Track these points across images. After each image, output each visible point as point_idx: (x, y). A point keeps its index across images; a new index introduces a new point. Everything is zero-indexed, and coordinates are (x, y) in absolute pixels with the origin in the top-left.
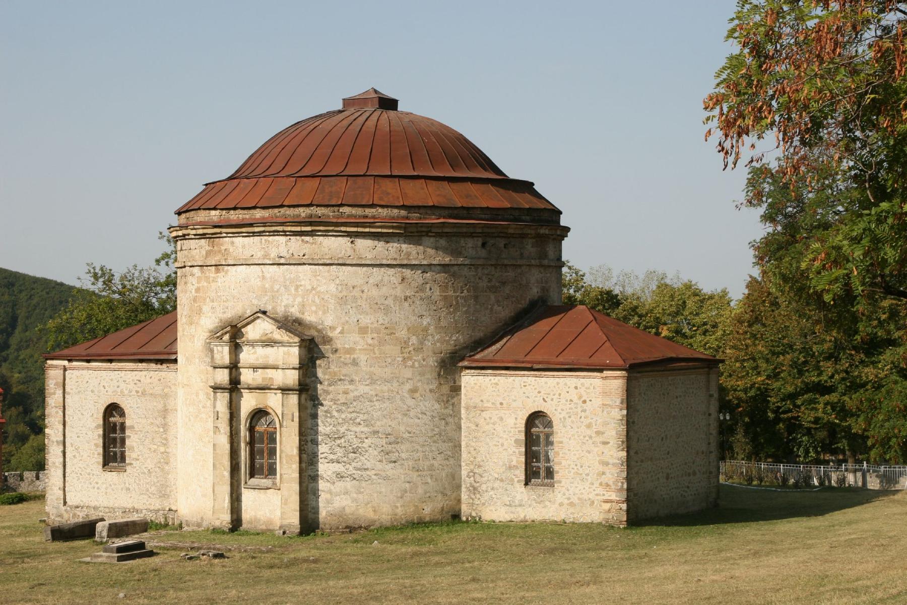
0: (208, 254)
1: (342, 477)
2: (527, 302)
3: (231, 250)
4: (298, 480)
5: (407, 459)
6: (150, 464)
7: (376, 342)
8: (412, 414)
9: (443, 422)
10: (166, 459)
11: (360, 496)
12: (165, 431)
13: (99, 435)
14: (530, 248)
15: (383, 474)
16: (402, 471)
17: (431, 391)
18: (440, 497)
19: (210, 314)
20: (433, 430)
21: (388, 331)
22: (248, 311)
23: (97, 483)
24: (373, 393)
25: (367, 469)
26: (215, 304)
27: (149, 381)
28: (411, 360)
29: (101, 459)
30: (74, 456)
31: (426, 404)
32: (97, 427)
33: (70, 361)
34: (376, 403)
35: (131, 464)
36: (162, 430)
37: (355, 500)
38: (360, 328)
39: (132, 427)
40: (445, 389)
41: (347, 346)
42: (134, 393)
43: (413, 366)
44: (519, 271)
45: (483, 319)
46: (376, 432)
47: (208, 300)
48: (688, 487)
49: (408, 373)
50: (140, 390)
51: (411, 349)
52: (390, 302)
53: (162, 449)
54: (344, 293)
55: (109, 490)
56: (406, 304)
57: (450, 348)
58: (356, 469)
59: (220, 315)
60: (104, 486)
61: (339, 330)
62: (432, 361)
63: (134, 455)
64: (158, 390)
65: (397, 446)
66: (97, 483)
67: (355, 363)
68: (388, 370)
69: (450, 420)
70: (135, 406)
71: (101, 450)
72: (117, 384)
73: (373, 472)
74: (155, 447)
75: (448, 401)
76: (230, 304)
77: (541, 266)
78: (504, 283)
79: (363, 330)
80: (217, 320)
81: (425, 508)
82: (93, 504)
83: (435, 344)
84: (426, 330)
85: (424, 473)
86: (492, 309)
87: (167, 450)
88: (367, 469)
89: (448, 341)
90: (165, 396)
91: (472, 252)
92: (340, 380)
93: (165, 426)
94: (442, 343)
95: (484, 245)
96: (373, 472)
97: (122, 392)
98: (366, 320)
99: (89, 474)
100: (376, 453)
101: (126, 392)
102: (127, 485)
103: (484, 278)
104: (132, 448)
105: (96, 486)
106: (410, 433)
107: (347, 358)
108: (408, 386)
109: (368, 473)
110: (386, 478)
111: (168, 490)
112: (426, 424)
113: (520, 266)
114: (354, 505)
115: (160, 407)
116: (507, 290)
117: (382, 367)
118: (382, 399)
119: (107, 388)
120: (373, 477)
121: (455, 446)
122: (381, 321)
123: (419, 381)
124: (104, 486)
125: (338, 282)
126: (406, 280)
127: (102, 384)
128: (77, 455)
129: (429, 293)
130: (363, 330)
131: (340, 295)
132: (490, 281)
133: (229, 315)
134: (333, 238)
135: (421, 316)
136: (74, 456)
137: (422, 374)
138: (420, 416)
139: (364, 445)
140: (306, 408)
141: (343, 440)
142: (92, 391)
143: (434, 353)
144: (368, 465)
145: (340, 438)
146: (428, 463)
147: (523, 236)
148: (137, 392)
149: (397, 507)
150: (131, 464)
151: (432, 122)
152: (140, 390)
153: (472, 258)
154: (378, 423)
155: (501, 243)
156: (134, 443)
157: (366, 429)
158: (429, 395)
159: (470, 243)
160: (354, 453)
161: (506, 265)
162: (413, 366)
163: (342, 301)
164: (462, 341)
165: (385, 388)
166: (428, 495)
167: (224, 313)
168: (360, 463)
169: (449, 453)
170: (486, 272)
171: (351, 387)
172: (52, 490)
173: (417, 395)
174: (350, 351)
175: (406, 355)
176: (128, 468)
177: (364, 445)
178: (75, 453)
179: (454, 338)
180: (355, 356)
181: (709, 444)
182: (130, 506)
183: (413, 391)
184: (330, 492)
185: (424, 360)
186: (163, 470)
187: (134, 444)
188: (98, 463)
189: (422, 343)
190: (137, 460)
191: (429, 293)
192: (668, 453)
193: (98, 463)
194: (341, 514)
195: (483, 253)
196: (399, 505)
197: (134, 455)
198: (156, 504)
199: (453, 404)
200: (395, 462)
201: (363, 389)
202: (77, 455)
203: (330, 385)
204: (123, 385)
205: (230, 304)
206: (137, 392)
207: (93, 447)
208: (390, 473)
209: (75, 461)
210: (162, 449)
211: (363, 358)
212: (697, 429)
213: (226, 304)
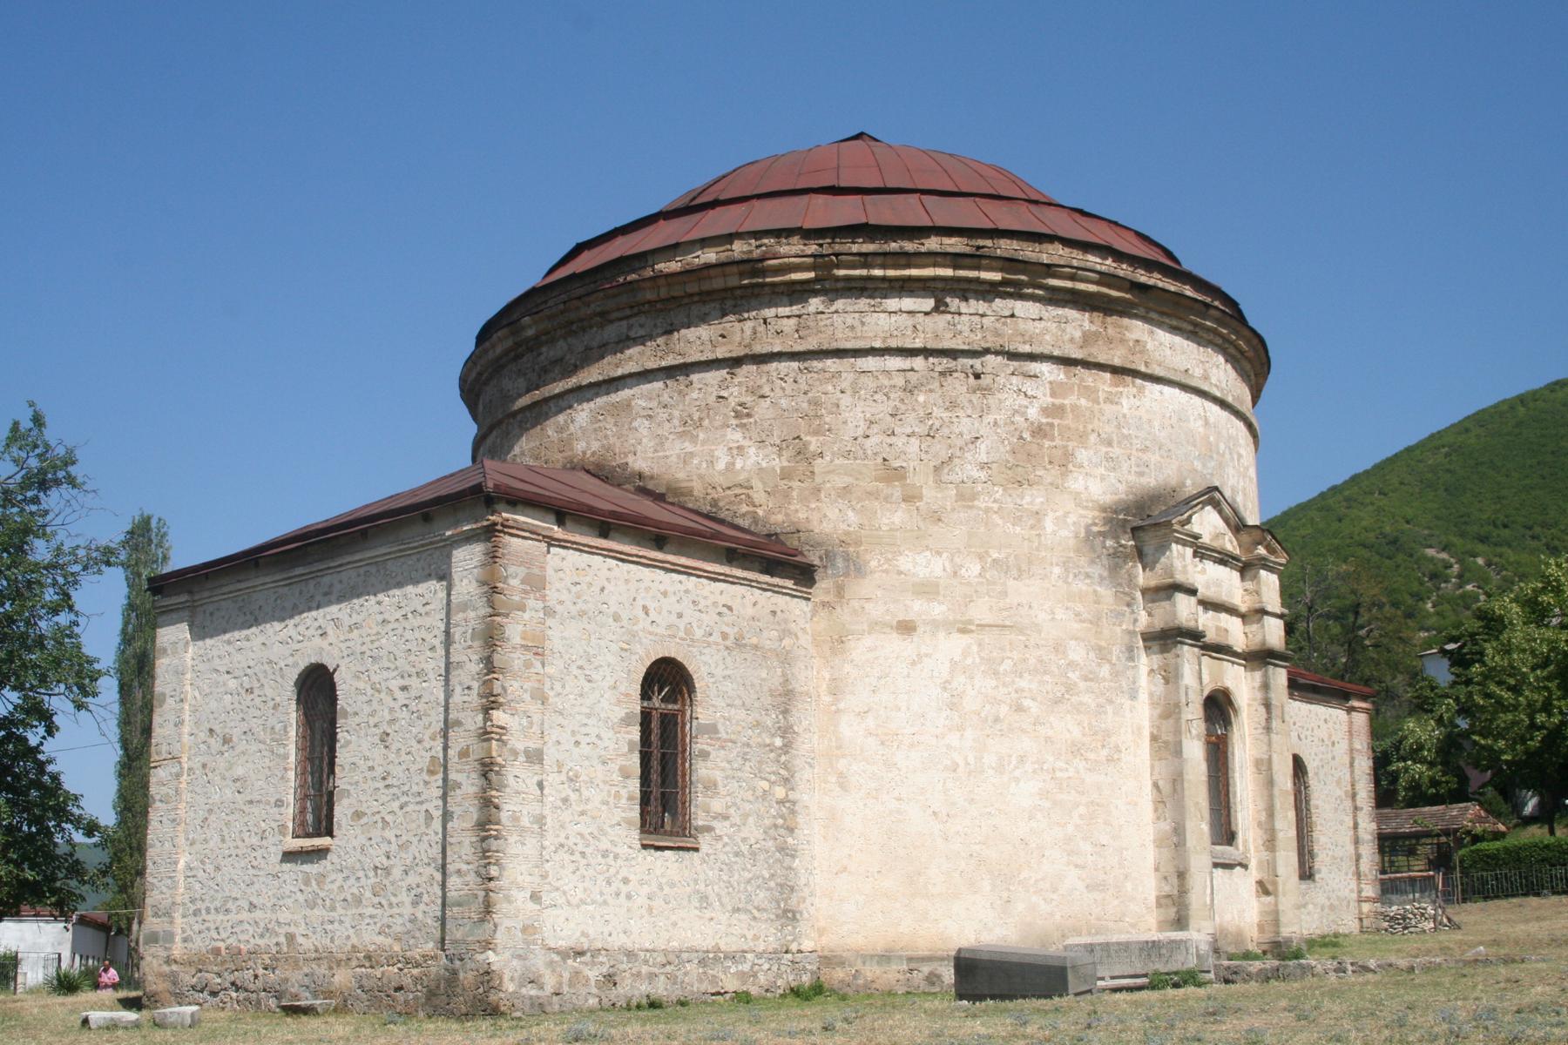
0: (1088, 339)
3: (1149, 346)
4: (1295, 844)
6: (753, 831)
10: (787, 818)
12: (787, 748)
13: (631, 743)
19: (1102, 470)
22: (1189, 482)
23: (626, 881)
26: (1116, 451)
27: (750, 611)
29: (635, 813)
30: (565, 800)
32: (626, 721)
33: (560, 522)
35: (709, 829)
36: (778, 742)
39: (712, 729)
42: (716, 637)
47: (1093, 438)
50: (732, 632)
53: (780, 792)
55: (658, 903)
59: (1132, 478)
60: (645, 890)
63: (717, 805)
64: (769, 639)
66: (626, 881)
70: (719, 672)
71: (634, 786)
72: (678, 608)
74: (765, 785)
76: (1154, 458)
80: (1122, 488)
82: (618, 941)
87: (792, 796)
90: (786, 658)
93: (786, 731)
97: (689, 630)
99: (605, 854)
101: (699, 633)
102: (702, 887)
104: (711, 786)
105: (624, 889)
111: (793, 902)
115: (776, 682)
119: (653, 615)
124: (645, 890)
127: (640, 602)
128: (573, 796)
133: (1151, 481)
136: (565, 800)
142: (617, 618)
148: (725, 636)
150: (709, 829)
152: (732, 632)
156: (718, 775)
167: (1141, 474)
172: (508, 899)
176: (704, 841)
178: (567, 791)
182: (708, 944)
186: (782, 849)
187: (718, 776)
188: (629, 822)
190: (726, 818)
193: (629, 822)
197: (717, 805)
198: (768, 936)
202: (573, 796)
204: (689, 613)
205: (1154, 458)
206: (725, 636)
207: (616, 777)
209: (566, 816)
210: (780, 792)
213: (1145, 457)
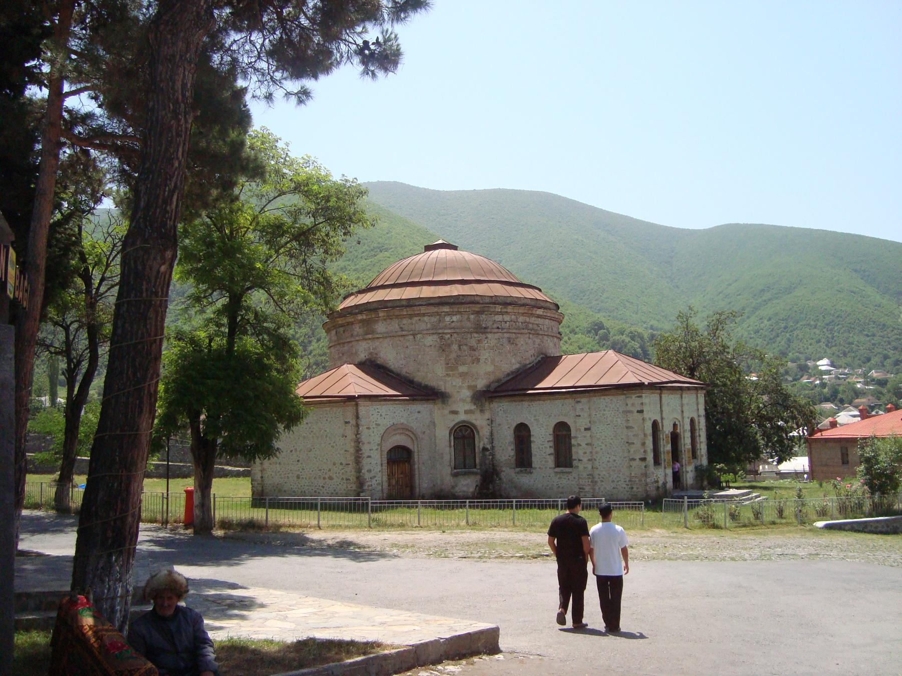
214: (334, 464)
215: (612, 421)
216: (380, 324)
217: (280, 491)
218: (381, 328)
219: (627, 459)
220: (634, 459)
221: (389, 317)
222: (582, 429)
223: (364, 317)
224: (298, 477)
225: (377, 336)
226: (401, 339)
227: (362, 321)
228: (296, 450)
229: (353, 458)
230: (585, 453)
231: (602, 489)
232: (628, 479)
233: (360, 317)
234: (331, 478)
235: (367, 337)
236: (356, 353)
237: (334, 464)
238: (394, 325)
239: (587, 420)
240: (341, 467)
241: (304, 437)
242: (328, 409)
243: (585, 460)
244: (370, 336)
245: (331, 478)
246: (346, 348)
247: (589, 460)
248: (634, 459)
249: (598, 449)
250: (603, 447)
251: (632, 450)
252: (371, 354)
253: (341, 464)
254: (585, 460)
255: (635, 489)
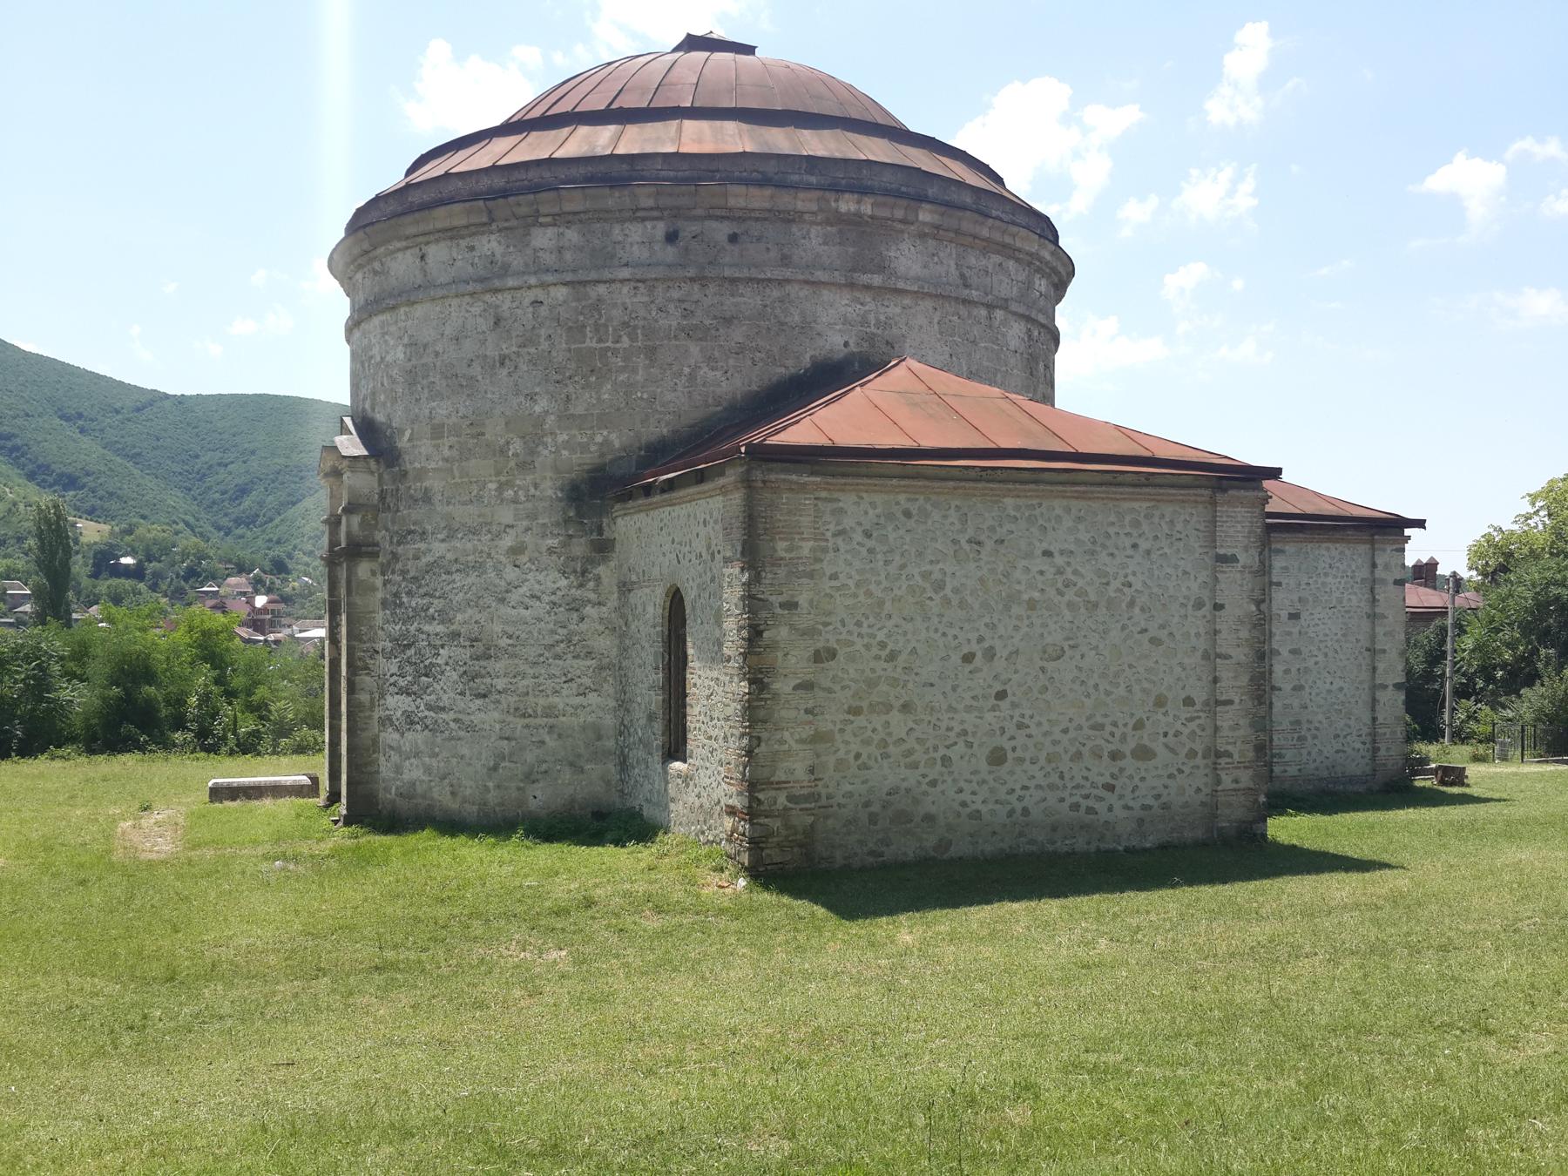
1: (412, 723)
2: (806, 361)
5: (504, 691)
7: (455, 453)
8: (514, 597)
9: (575, 615)
11: (434, 762)
14: (814, 242)
15: (465, 718)
16: (496, 715)
17: (551, 551)
18: (567, 775)
20: (553, 632)
21: (474, 431)
24: (450, 556)
25: (443, 709)
28: (513, 487)
31: (541, 577)
34: (457, 577)
37: (428, 770)
38: (433, 428)
40: (580, 548)
41: (417, 465)
43: (515, 501)
44: (776, 293)
45: (669, 396)
46: (455, 635)
48: (1110, 788)
49: (506, 515)
51: (512, 464)
52: (476, 370)
54: (414, 362)
56: (505, 372)
57: (590, 458)
58: (429, 707)
61: (407, 434)
62: (549, 489)
65: (491, 665)
67: (427, 498)
68: (471, 509)
69: (588, 610)
73: (452, 715)
75: (583, 573)
77: (852, 286)
78: (728, 321)
79: (437, 432)
81: (538, 794)
83: (557, 452)
84: (539, 421)
85: (539, 721)
86: (692, 377)
88: (443, 709)
89: (584, 448)
91: (640, 253)
92: (410, 532)
94: (573, 451)
95: (671, 237)
96: (452, 715)
98: (442, 410)
100: (455, 676)
103: (671, 307)
106: (510, 637)
107: (416, 487)
108: (508, 541)
109: (444, 716)
110: (470, 728)
112: (539, 620)
113: (788, 281)
114: (426, 778)
116: (738, 334)
117: (464, 504)
118: (465, 569)
120: (452, 725)
121: (602, 668)
122: (462, 411)
123: (528, 529)
125: (406, 340)
126: (503, 323)
129: (545, 345)
130: (437, 432)
131: (409, 366)
132: (687, 313)
134: (400, 255)
135: (532, 397)
137: (533, 516)
138: (530, 602)
139: (440, 661)
140: (374, 589)
141: (413, 651)
143: (556, 470)
144: (445, 701)
145: (409, 646)
146: (542, 701)
147: (789, 218)
149: (487, 789)
151: (850, 89)
153: (637, 265)
154: (459, 617)
155: (722, 230)
157: (440, 629)
158: (545, 558)
159: (636, 232)
160: (427, 675)
161: (733, 281)
162: (515, 501)
163: (412, 377)
164: (617, 444)
165: (469, 546)
166: (544, 767)
168: (433, 697)
169: (587, 681)
170: (676, 294)
171: (423, 546)
173: (523, 559)
174: (421, 474)
175: (503, 479)
177: (440, 661)
179: (599, 439)
180: (427, 484)
181: (1215, 680)
183: (516, 550)
184: (398, 750)
185: (536, 486)
189: (532, 452)
191: (545, 345)
192: (1001, 695)
194: (408, 794)
195: (670, 253)
196: (491, 784)
199: (598, 579)
200: (485, 696)
201: (439, 548)
203: (399, 543)
208: (477, 718)
211: (435, 484)
212: (1155, 641)
214: (1160, 702)
215: (1340, 601)
216: (904, 246)
217: (903, 817)
218: (907, 258)
219: (1366, 686)
220: (1385, 687)
221: (935, 233)
222: (1284, 614)
223: (867, 208)
224: (997, 757)
225: (901, 285)
226: (963, 311)
227: (840, 219)
228: (990, 654)
229: (1244, 680)
230: (1287, 672)
231: (1314, 755)
232: (1365, 730)
233: (847, 204)
234: (1144, 753)
235: (865, 278)
236: (806, 327)
237: (1160, 702)
238: (947, 264)
239: (1295, 597)
240: (1186, 713)
241: (1032, 605)
242: (1143, 506)
243: (1287, 687)
244: (877, 280)
245: (1144, 753)
246: (749, 299)
247: (1294, 689)
248: (1385, 687)
249: (1310, 663)
250: (1320, 658)
251: (1381, 666)
252: (871, 338)
253: (1189, 702)
254: (1287, 687)
255: (1382, 752)
